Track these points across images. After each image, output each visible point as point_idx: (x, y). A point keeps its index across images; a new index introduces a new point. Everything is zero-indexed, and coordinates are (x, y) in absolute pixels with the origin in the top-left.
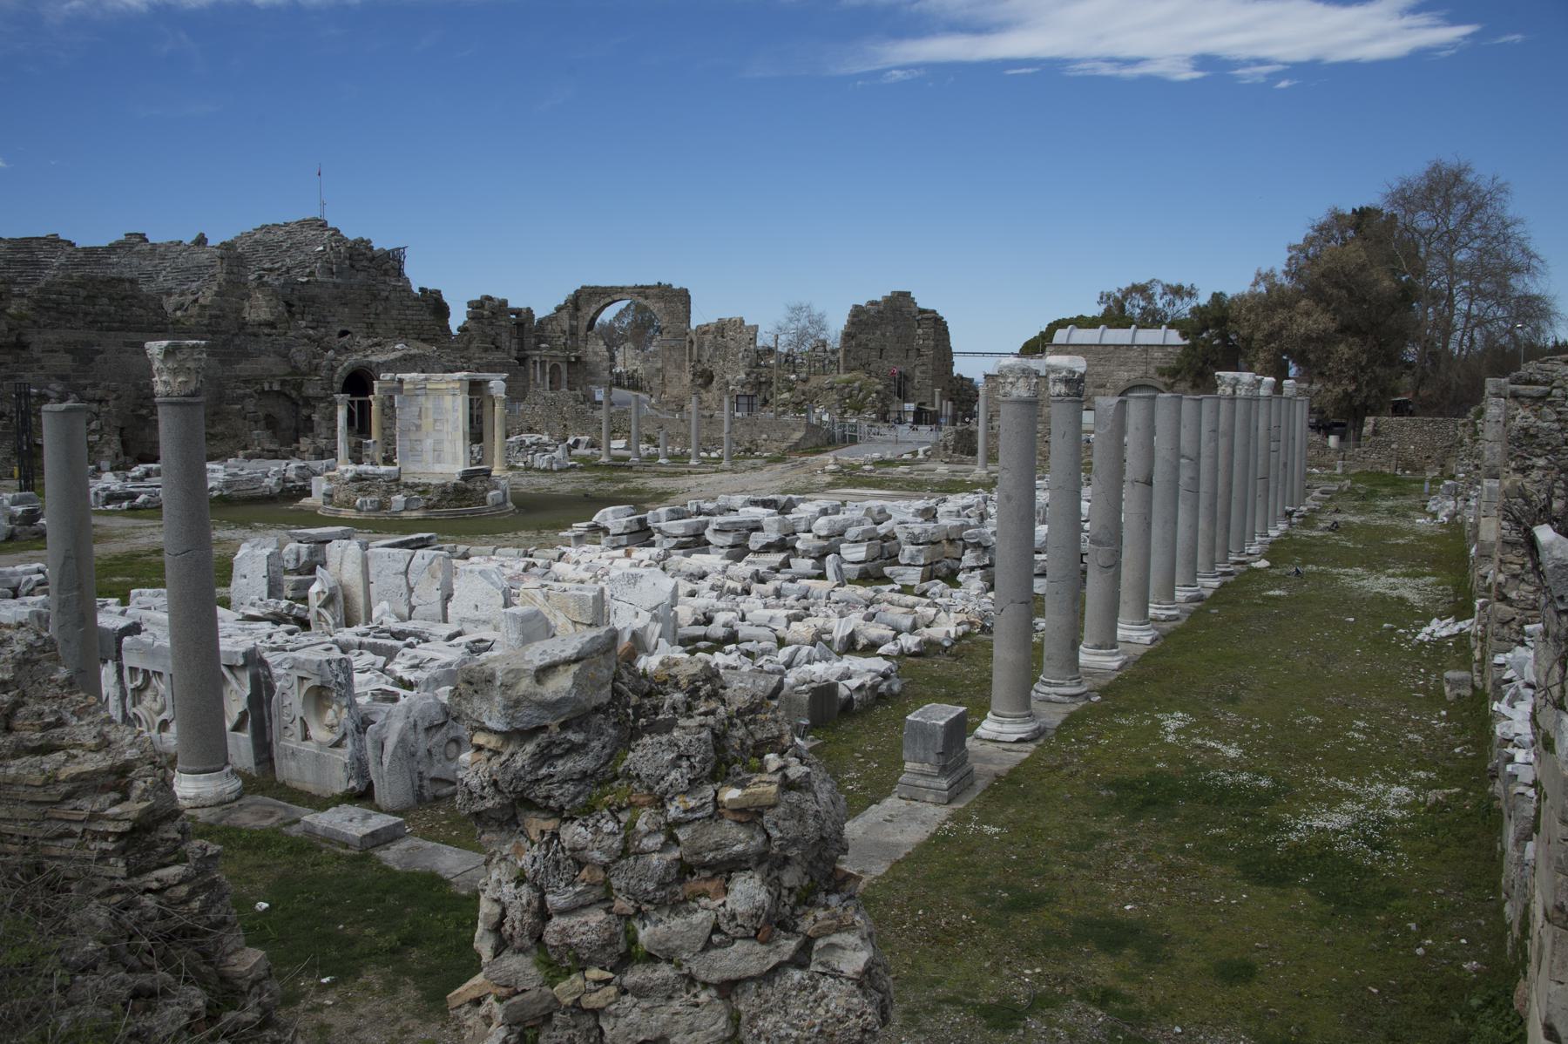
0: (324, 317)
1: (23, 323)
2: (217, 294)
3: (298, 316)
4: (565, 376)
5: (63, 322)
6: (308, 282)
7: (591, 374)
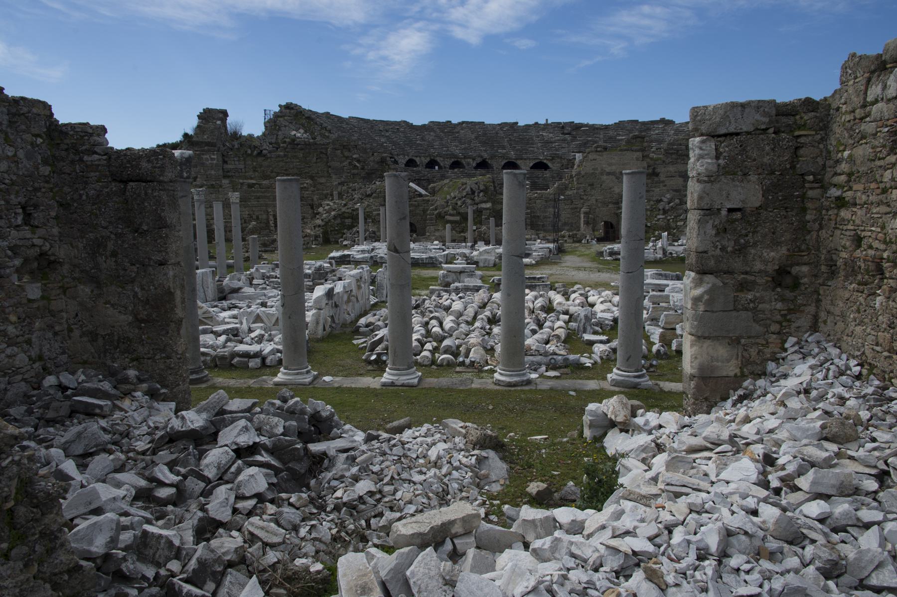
5: (679, 161)
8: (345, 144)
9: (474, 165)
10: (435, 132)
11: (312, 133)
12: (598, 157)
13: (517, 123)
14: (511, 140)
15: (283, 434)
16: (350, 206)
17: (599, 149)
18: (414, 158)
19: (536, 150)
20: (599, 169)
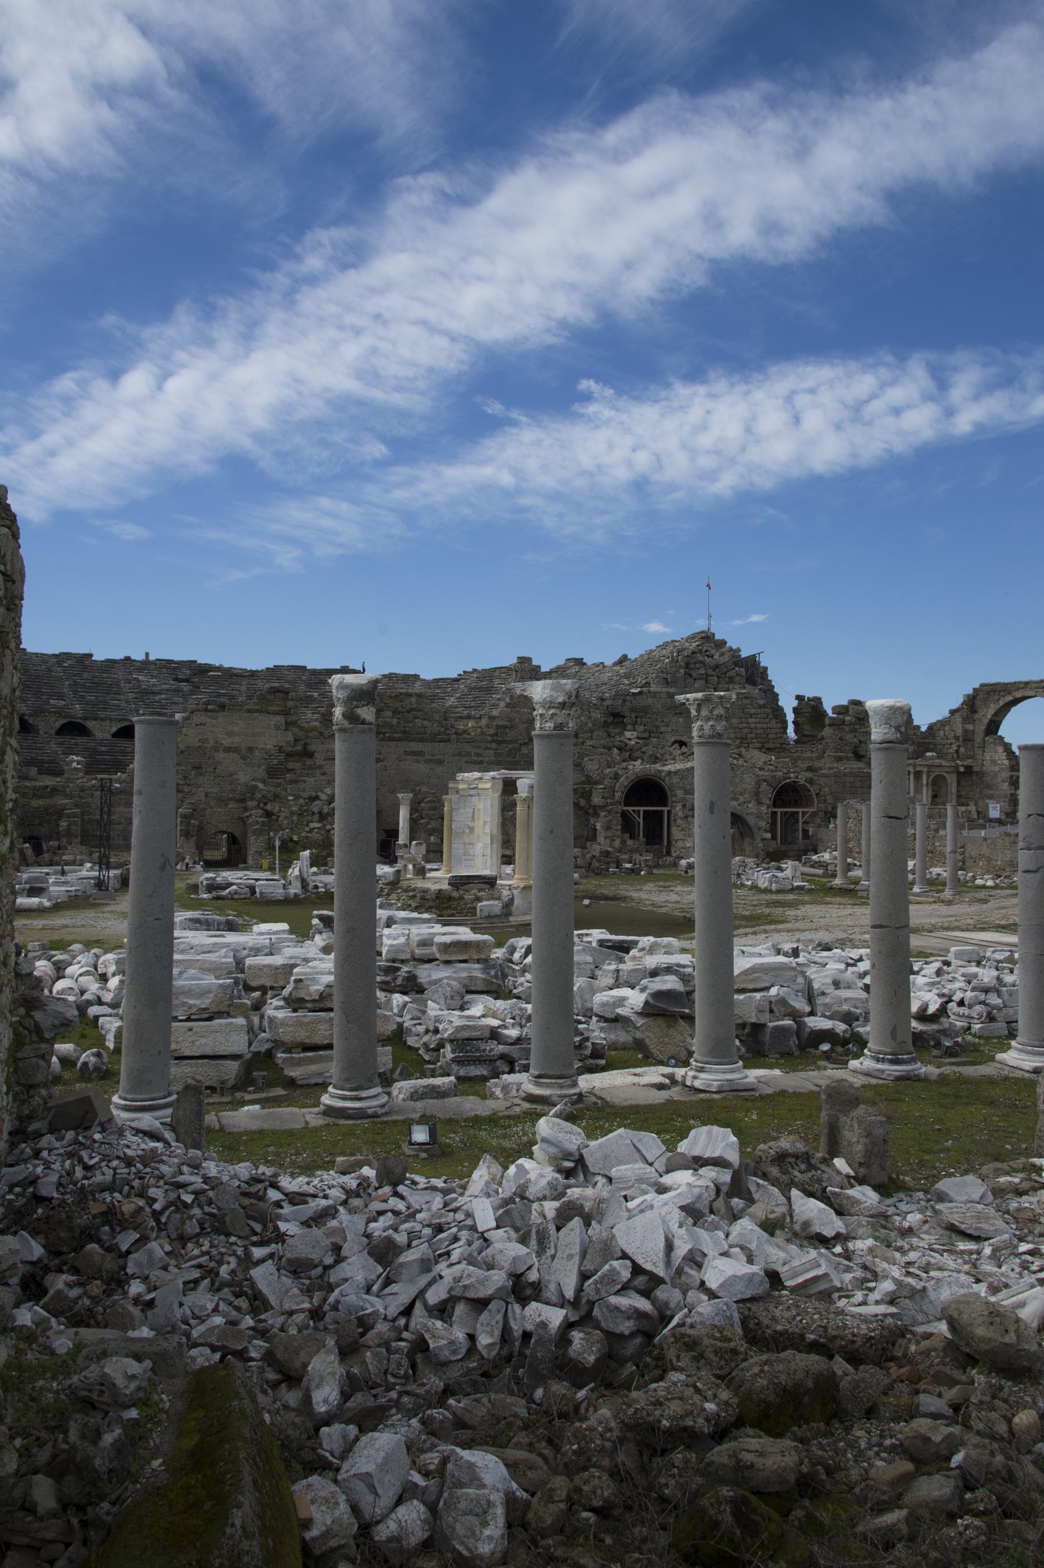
0: (657, 727)
1: (310, 735)
2: (507, 706)
3: (629, 727)
4: (954, 788)
6: (640, 693)
7: (989, 787)
12: (209, 720)
14: (76, 683)
17: (210, 707)
19: (123, 704)
20: (211, 741)
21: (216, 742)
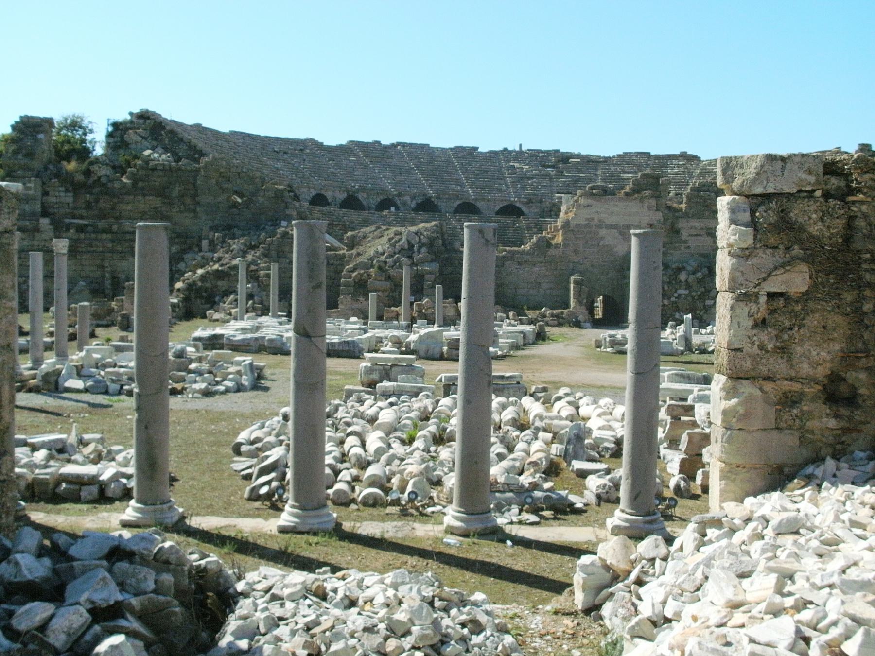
8: (222, 170)
9: (413, 205)
10: (356, 156)
11: (174, 154)
13: (477, 148)
15: (155, 592)
16: (227, 260)
18: (323, 193)
20: (596, 220)
21: (600, 221)
